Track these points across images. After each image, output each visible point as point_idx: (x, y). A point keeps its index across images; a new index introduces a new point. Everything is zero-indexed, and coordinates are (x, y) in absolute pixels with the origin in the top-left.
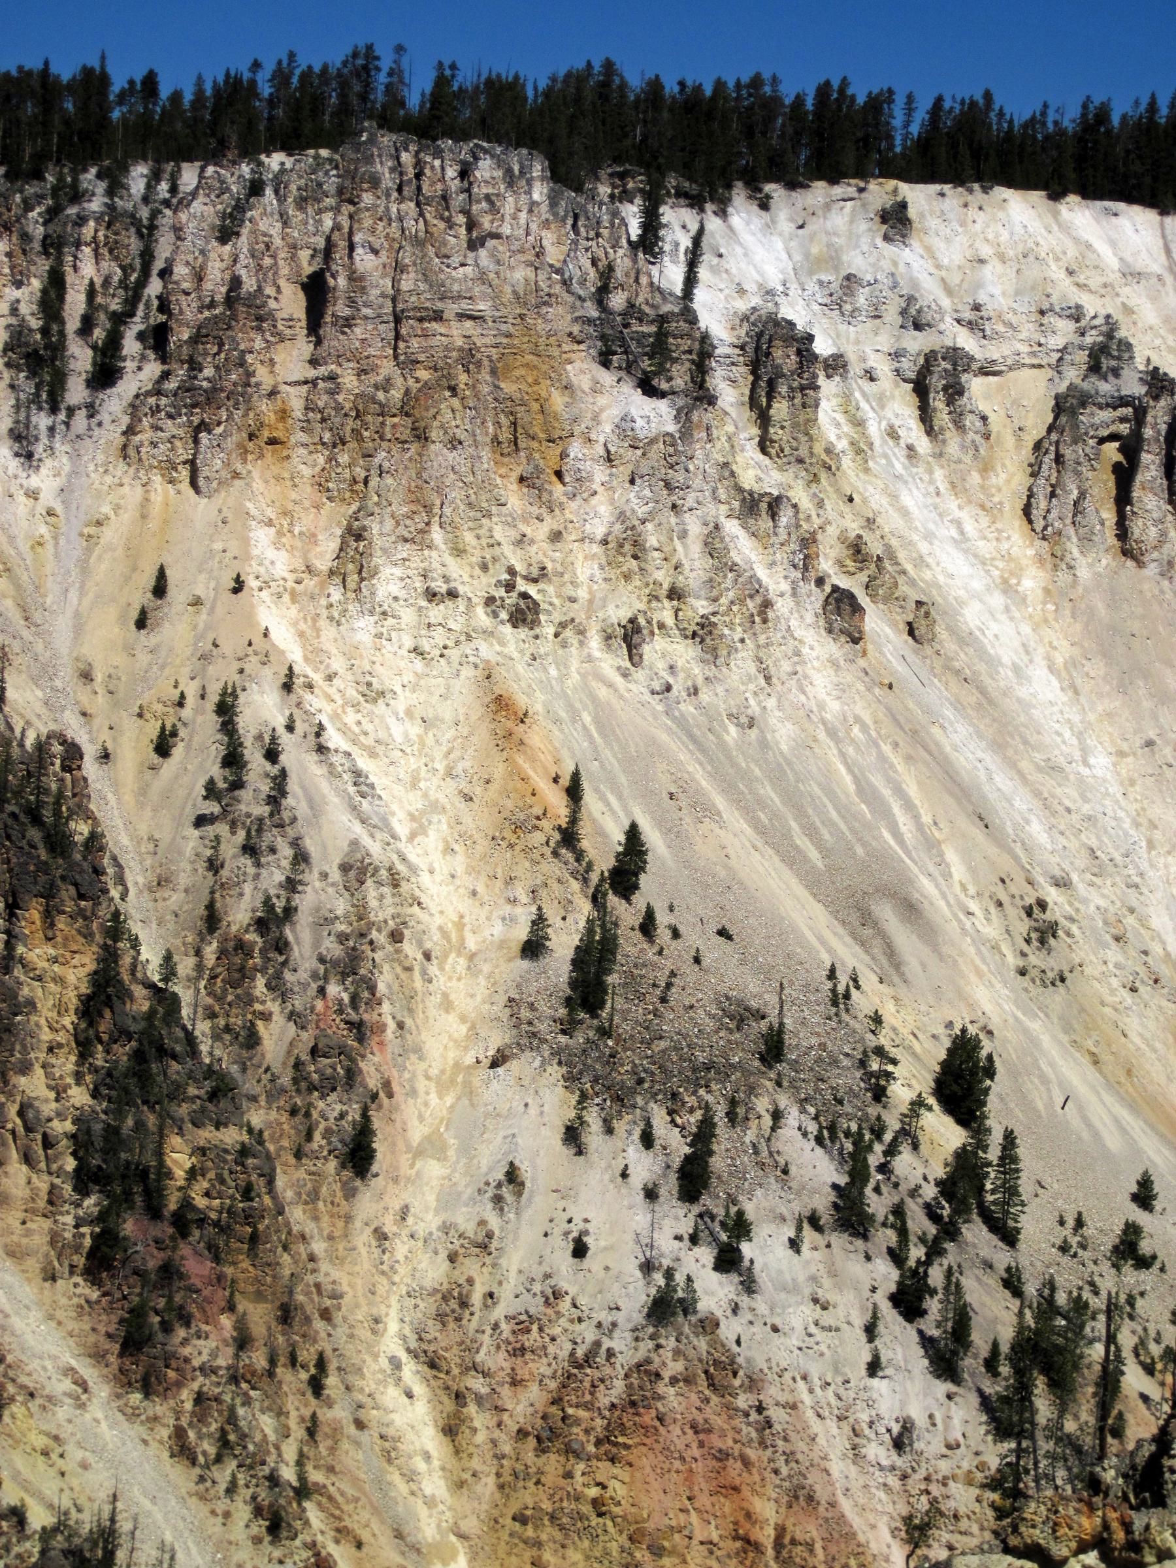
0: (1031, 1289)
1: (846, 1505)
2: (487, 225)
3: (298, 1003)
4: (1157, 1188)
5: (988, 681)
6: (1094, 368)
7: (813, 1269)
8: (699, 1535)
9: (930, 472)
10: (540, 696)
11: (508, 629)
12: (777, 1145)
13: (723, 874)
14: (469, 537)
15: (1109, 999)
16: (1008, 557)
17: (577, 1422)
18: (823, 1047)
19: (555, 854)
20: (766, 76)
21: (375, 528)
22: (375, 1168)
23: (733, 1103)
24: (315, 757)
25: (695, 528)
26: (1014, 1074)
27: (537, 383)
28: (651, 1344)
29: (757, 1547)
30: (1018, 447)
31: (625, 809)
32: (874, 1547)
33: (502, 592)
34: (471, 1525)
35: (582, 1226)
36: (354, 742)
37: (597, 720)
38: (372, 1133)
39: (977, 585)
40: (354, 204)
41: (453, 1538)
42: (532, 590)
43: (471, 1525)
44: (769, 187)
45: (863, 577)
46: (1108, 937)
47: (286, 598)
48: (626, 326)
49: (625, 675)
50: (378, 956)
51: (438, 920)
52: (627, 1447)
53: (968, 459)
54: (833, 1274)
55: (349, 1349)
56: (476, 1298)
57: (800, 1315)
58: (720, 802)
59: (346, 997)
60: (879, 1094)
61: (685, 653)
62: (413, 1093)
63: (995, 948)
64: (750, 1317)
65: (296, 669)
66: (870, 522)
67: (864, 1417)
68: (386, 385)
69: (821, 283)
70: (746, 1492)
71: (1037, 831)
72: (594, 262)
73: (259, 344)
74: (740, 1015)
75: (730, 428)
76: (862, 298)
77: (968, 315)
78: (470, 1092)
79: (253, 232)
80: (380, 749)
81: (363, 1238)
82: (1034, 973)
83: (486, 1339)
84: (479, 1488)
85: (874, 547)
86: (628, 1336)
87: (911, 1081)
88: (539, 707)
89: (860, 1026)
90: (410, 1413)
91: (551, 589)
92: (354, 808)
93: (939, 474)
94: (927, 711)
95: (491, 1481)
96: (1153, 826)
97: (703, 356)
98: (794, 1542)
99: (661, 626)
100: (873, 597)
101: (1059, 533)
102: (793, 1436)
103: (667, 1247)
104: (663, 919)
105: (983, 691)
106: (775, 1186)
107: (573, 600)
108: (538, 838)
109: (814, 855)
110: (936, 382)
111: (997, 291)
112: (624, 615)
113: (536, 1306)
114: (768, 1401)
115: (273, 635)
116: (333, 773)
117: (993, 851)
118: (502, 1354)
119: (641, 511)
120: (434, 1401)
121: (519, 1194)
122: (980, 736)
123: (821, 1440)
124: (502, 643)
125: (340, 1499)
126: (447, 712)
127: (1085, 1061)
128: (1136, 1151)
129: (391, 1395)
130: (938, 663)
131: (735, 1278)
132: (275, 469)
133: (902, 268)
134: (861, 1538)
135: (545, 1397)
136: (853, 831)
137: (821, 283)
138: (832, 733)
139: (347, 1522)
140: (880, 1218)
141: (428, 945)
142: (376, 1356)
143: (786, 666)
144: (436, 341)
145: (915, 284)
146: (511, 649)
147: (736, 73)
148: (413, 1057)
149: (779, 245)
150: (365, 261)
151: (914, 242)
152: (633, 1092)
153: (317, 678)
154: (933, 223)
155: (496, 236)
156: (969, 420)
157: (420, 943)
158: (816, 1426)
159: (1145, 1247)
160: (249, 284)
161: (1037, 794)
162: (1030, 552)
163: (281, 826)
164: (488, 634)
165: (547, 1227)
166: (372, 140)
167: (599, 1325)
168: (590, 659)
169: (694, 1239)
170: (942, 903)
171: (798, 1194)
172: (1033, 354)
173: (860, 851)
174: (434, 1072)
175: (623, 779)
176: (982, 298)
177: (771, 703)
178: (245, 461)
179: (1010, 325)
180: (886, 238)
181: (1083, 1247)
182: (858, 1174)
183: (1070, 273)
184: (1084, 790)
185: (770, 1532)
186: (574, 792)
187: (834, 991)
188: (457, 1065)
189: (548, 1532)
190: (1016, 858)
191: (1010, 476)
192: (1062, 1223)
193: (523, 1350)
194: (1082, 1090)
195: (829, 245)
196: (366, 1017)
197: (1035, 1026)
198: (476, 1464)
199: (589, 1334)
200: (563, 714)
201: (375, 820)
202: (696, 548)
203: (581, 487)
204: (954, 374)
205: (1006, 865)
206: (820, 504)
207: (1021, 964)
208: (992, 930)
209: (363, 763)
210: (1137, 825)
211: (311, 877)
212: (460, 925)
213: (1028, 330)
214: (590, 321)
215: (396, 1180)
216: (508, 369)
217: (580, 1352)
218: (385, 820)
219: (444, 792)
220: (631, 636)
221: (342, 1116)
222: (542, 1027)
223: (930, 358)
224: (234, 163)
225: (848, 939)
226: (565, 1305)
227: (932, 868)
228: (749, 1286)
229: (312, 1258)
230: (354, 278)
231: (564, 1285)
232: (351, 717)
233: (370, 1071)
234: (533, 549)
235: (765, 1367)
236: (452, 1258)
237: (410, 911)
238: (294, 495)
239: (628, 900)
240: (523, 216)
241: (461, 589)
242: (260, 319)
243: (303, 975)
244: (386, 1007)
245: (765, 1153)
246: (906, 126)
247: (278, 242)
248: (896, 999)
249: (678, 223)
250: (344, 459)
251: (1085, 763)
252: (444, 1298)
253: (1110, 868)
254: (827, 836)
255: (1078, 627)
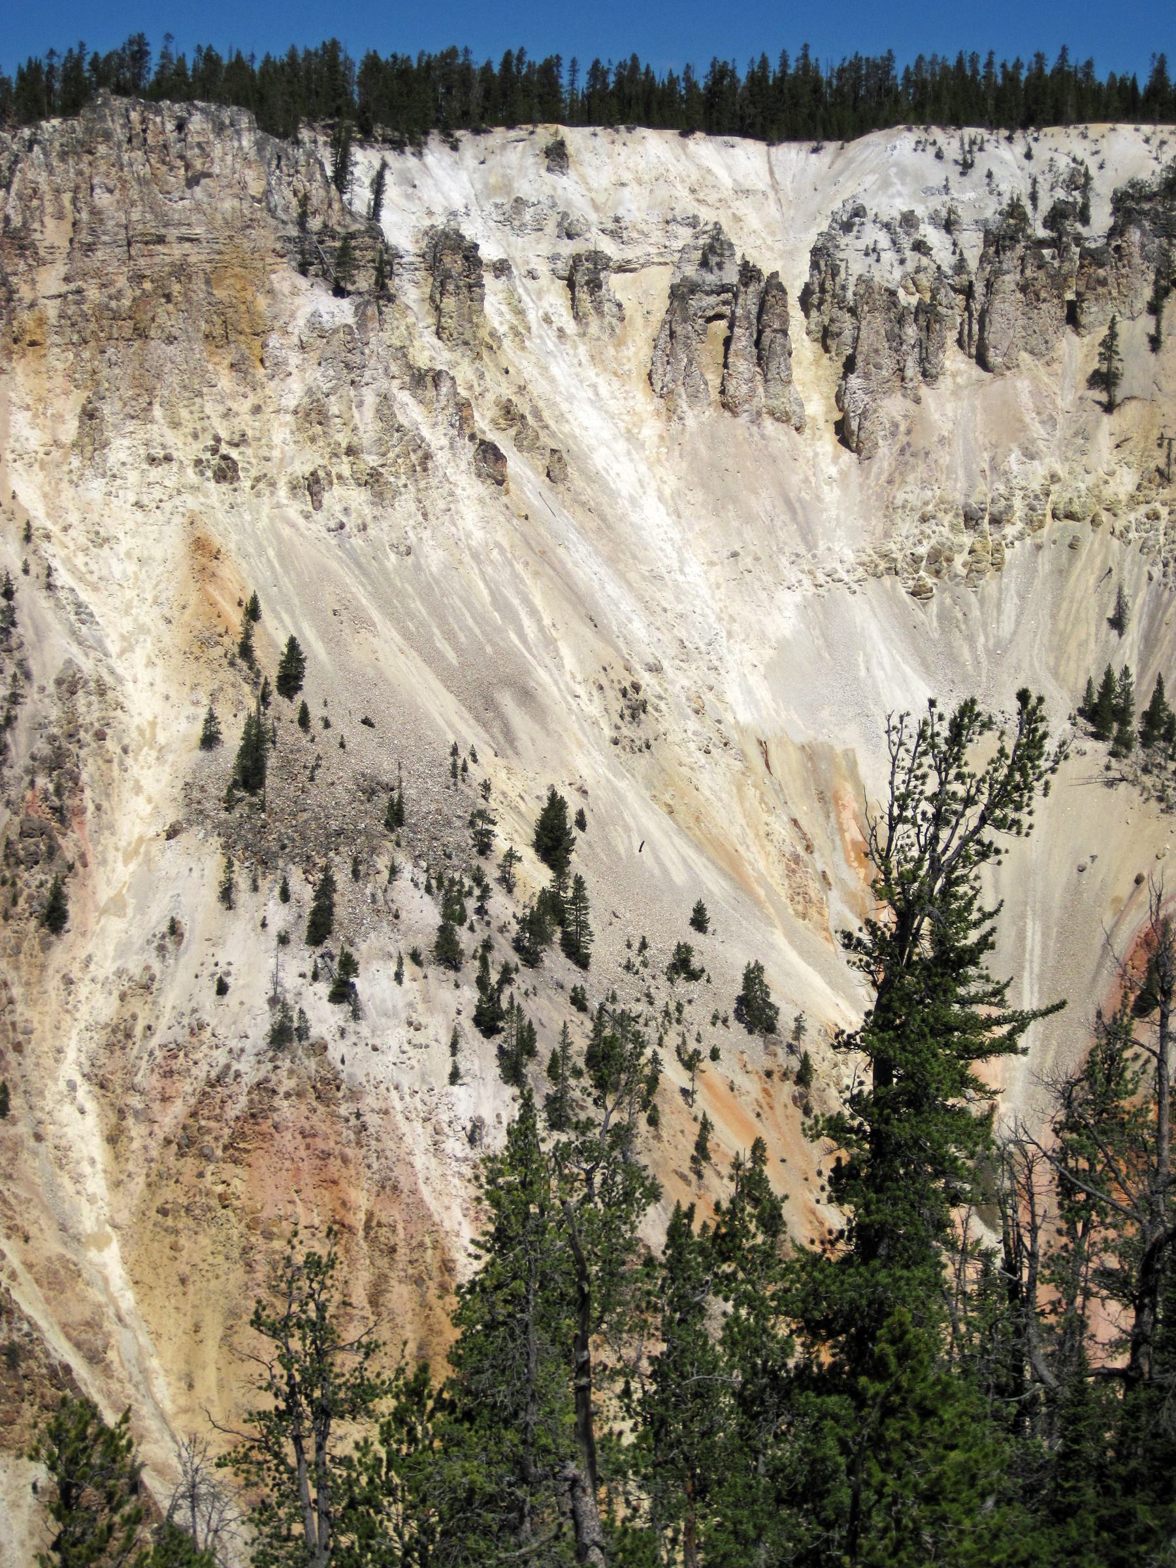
0: (594, 1004)
1: (426, 1192)
2: (199, 167)
3: (13, 793)
4: (708, 914)
5: (608, 511)
6: (704, 264)
7: (410, 997)
8: (303, 1222)
9: (575, 348)
10: (235, 537)
11: (212, 484)
12: (392, 894)
13: (371, 673)
14: (184, 413)
15: (686, 760)
16: (631, 412)
17: (209, 1131)
18: (439, 811)
19: (232, 664)
20: (460, 48)
21: (106, 409)
22: (67, 926)
23: (356, 862)
24: (45, 593)
25: (370, 398)
26: (602, 825)
27: (244, 289)
28: (270, 1066)
29: (351, 1229)
30: (646, 326)
31: (296, 624)
32: (447, 1225)
33: (208, 455)
34: (123, 1217)
35: (225, 968)
36: (81, 579)
37: (281, 556)
38: (66, 897)
39: (606, 435)
40: (90, 153)
41: (108, 1229)
42: (234, 454)
43: (123, 1217)
44: (459, 134)
45: (512, 432)
46: (689, 711)
47: (36, 466)
48: (321, 242)
49: (307, 517)
50: (83, 753)
51: (137, 720)
52: (247, 1151)
53: (605, 337)
54: (426, 1000)
55: (34, 1076)
56: (138, 1030)
57: (396, 1036)
58: (375, 615)
59: (51, 787)
60: (484, 848)
61: (358, 497)
62: (104, 862)
63: (595, 723)
64: (354, 1039)
65: (34, 525)
66: (522, 389)
67: (445, 1117)
68: (119, 296)
69: (496, 206)
70: (343, 1184)
71: (638, 628)
72: (295, 194)
73: (22, 267)
74: (370, 789)
75: (411, 320)
76: (528, 215)
77: (610, 226)
78: (148, 860)
79: (23, 180)
80: (102, 584)
81: (53, 983)
82: (626, 742)
83: (144, 1064)
84: (131, 1186)
85: (524, 408)
86: (253, 1059)
87: (513, 834)
88: (232, 546)
89: (473, 792)
90: (80, 1126)
91: (249, 451)
92: (74, 633)
93: (582, 350)
94: (556, 536)
95: (141, 1180)
96: (732, 619)
97: (385, 263)
98: (379, 1225)
99: (340, 477)
100: (520, 448)
101: (671, 392)
102: (384, 1137)
103: (290, 981)
104: (316, 713)
105: (603, 519)
106: (385, 927)
107: (267, 459)
108: (219, 651)
109: (451, 655)
110: (580, 278)
111: (633, 207)
112: (307, 469)
113: (182, 1036)
114: (364, 1108)
115: (21, 497)
116: (59, 606)
117: (599, 646)
118: (156, 1076)
119: (325, 388)
120: (102, 1115)
121: (179, 943)
122: (598, 553)
123: (408, 1139)
124: (207, 496)
125: (13, 1201)
126: (158, 554)
127: (662, 812)
128: (696, 882)
129: (67, 1112)
130: (568, 497)
131: (346, 1008)
132: (34, 365)
133: (560, 191)
134: (436, 1218)
135: (187, 1110)
136: (484, 633)
137: (496, 206)
138: (475, 556)
139: (18, 1221)
140: (469, 952)
141: (126, 741)
142: (56, 1080)
143: (441, 505)
144: (157, 260)
145: (569, 203)
146: (214, 500)
147: (435, 49)
148: (107, 833)
149: (464, 176)
150: (102, 199)
151: (571, 172)
152: (276, 856)
153: (55, 530)
154: (587, 156)
155: (209, 175)
156: (607, 307)
157: (120, 740)
158: (404, 1126)
159: (696, 963)
160: (16, 221)
161: (640, 598)
162: (651, 408)
163: (9, 650)
164: (195, 489)
165: (198, 970)
166: (105, 103)
167: (231, 1051)
168: (278, 506)
169: (315, 977)
170: (554, 689)
171: (405, 935)
172: (661, 254)
173: (489, 649)
174: (122, 844)
175: (296, 601)
176: (621, 212)
177: (426, 534)
178: (10, 360)
179: (642, 233)
180: (549, 169)
181: (645, 964)
182: (453, 915)
183: (693, 191)
184: (679, 594)
185: (362, 1216)
186: (253, 613)
187: (454, 765)
188: (141, 839)
189: (184, 1222)
190: (617, 650)
191: (638, 349)
192: (629, 946)
193: (171, 1072)
194: (656, 834)
195: (504, 176)
196: (69, 802)
197: (622, 785)
198: (131, 1167)
199: (221, 1057)
200: (251, 550)
201: (91, 642)
202: (369, 411)
203: (278, 370)
204: (596, 271)
205: (608, 655)
206: (481, 376)
207: (614, 734)
208: (593, 709)
209: (84, 596)
210: (720, 619)
211: (31, 693)
212: (153, 724)
213: (657, 236)
214: (289, 239)
215: (84, 934)
216: (221, 279)
217: (213, 1075)
218: (100, 642)
219: (149, 616)
220: (313, 486)
221: (41, 885)
222: (208, 805)
223: (577, 259)
224: (14, 128)
225: (472, 722)
226: (206, 1035)
227: (548, 661)
228: (356, 1015)
229: (11, 1001)
230: (95, 212)
231: (206, 1018)
232: (80, 560)
233: (68, 846)
234: (236, 421)
235: (364, 1080)
236: (123, 997)
237: (112, 714)
238: (48, 385)
239: (291, 698)
240: (229, 158)
241: (175, 454)
242: (22, 247)
243: (18, 770)
244: (88, 793)
245: (381, 901)
246: (575, 83)
247: (44, 187)
248: (509, 770)
249: (364, 161)
250: (86, 355)
251: (682, 571)
252: (114, 1032)
253: (696, 655)
254: (463, 639)
255: (684, 465)
